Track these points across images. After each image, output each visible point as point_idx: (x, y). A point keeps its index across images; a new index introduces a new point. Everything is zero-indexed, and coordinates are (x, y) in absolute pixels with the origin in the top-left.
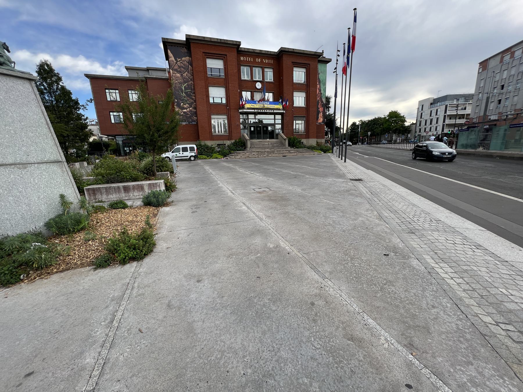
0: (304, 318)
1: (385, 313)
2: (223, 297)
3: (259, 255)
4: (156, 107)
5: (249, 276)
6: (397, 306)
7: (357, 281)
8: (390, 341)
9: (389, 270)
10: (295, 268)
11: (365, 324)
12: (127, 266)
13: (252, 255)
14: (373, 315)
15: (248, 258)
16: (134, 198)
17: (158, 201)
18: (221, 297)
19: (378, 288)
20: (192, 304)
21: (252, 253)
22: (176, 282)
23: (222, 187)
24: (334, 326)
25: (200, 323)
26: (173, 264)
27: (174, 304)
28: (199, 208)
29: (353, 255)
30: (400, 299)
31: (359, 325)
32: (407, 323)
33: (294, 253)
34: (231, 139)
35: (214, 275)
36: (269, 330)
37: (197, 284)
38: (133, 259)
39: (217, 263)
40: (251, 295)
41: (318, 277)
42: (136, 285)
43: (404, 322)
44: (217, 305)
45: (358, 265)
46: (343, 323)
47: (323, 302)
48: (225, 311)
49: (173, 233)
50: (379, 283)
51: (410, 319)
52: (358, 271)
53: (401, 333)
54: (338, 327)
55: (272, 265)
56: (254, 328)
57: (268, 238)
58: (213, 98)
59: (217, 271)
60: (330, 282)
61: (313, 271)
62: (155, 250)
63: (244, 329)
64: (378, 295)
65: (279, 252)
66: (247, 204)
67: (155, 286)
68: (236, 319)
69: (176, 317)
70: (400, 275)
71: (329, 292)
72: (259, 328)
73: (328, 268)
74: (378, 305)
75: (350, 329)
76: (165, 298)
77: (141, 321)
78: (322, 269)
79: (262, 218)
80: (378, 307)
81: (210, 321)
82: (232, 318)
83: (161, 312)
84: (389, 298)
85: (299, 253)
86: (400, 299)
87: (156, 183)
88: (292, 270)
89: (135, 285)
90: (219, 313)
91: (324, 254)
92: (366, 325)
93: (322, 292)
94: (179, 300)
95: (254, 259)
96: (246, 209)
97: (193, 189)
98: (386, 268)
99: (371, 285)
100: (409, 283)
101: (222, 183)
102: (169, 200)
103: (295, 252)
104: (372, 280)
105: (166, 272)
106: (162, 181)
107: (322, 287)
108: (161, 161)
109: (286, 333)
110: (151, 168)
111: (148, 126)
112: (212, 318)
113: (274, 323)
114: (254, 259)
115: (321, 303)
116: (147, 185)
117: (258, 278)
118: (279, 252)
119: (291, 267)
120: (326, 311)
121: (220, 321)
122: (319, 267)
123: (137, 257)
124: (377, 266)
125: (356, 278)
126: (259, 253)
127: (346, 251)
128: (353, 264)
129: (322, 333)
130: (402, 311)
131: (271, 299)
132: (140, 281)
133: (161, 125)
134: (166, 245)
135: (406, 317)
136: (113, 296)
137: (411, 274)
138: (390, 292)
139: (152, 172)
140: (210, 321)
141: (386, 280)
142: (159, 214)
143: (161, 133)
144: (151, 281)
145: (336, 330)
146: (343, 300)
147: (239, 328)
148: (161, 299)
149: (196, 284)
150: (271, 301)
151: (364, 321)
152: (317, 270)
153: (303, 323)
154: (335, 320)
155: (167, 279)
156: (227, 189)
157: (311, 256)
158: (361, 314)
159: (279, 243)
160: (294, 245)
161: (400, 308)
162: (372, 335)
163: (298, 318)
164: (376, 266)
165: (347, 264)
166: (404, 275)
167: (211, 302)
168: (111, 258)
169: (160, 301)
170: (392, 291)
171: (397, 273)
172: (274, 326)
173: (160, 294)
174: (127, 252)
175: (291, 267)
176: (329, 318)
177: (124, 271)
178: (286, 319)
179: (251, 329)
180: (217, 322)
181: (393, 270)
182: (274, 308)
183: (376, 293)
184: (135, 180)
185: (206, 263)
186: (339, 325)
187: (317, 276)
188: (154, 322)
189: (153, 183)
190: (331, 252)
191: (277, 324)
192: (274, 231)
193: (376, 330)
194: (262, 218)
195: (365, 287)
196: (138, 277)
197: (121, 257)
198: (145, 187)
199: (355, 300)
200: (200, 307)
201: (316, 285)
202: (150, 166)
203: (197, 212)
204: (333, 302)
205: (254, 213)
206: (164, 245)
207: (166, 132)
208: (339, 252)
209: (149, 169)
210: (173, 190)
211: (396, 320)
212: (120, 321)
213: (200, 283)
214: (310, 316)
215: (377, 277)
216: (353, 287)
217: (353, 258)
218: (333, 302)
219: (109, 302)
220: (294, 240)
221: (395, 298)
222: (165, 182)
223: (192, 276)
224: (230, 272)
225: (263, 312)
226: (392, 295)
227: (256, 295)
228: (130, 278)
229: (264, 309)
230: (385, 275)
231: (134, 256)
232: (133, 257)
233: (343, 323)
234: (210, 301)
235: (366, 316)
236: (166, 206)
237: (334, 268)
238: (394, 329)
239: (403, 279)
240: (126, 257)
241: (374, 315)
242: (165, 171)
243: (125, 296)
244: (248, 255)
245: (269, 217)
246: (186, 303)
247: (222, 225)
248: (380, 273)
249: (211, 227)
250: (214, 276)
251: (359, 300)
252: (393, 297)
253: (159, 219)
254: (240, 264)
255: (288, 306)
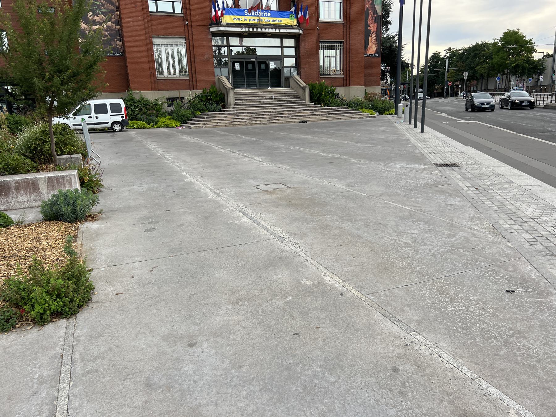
0: (383, 391)
1: (514, 378)
2: (240, 367)
3: (290, 298)
4: (52, 24)
5: (279, 333)
6: (534, 367)
7: (465, 334)
8: (525, 415)
9: (517, 314)
10: (357, 317)
11: (484, 395)
12: (49, 328)
13: (278, 300)
14: (496, 381)
15: (271, 304)
16: (20, 207)
17: (74, 211)
18: (237, 366)
19: (501, 342)
20: (190, 380)
21: (276, 295)
22: (150, 349)
23: (192, 183)
24: (434, 400)
25: (212, 408)
26: (136, 320)
27: (157, 382)
28: (156, 222)
29: (454, 294)
30: (536, 357)
31: (475, 396)
32: (549, 390)
33: (351, 294)
34: (348, 84)
35: (215, 334)
36: (330, 410)
37: (191, 350)
38: (58, 315)
39: (217, 315)
40: (289, 362)
41: (399, 330)
42: (77, 356)
43: (544, 389)
44: (234, 380)
45: (464, 308)
46: (448, 395)
47: (412, 366)
48: (249, 388)
49: (120, 268)
50: (501, 334)
51: (553, 383)
52: (466, 317)
53: (540, 403)
54: (441, 401)
55: (317, 314)
56: (305, 409)
57: (299, 271)
58: (173, 2)
59: (221, 327)
60: (419, 337)
61: (388, 320)
62: (94, 298)
63: (289, 411)
64: (502, 353)
65: (323, 292)
66: (249, 212)
67: (114, 357)
68: (271, 399)
69: (167, 401)
70: (536, 321)
71: (420, 351)
72: (313, 409)
73: (413, 315)
74: (502, 367)
75: (461, 402)
76: (138, 374)
77: (106, 411)
78: (404, 318)
79: (282, 236)
80: (503, 370)
81: (228, 403)
82: (264, 397)
83: (138, 396)
84: (519, 356)
85: (359, 294)
86: (536, 357)
87: (63, 177)
88: (353, 320)
89: (76, 356)
90: (240, 392)
91: (403, 294)
92: (486, 396)
93: (408, 351)
94: (164, 376)
95: (282, 305)
96: (249, 221)
97: (135, 187)
98: (512, 312)
99: (489, 339)
100: (550, 333)
101: (190, 175)
102: (95, 209)
103: (352, 291)
104: (490, 331)
105: (127, 333)
106: (75, 172)
107: (407, 345)
108: (61, 134)
109: (358, 413)
110: (40, 146)
111: (40, 62)
112: (229, 398)
113: (336, 401)
114: (282, 305)
115: (409, 367)
116: (45, 181)
117: (296, 335)
118: (323, 292)
119: (349, 316)
120: (419, 379)
121: (245, 403)
122: (398, 314)
123: (66, 312)
124: (496, 309)
125: (463, 329)
126: (290, 296)
127: (442, 287)
128: (455, 307)
129: (417, 411)
130: (541, 373)
131: (324, 366)
132: (84, 351)
133: (66, 60)
134: (112, 289)
135: (547, 382)
136: (41, 377)
137: (552, 319)
138: (521, 347)
139: (42, 154)
140: (228, 403)
141: (513, 330)
142: (80, 235)
143: (65, 75)
144: (103, 349)
145: (439, 404)
146: (445, 361)
147: (280, 410)
148: (131, 376)
149: (187, 349)
150: (325, 368)
151: (481, 390)
152: (396, 319)
153: (385, 398)
154: (436, 391)
155: (133, 344)
156: (203, 187)
157: (382, 298)
158: (476, 380)
159: (322, 278)
160: (349, 280)
161: (537, 369)
162: (496, 409)
163: (375, 391)
164: (495, 310)
165: (445, 307)
166: (542, 321)
167: (222, 375)
168: (15, 314)
169: (130, 379)
170: (524, 346)
171: (530, 319)
172: (337, 405)
173: (126, 368)
174: (46, 302)
175: (349, 316)
176: (425, 388)
177: (45, 335)
178: (355, 393)
179: (300, 410)
180: (240, 405)
181: (523, 314)
182: (332, 379)
183: (497, 349)
184: (14, 171)
185: (197, 315)
186: (442, 397)
187: (396, 328)
188: (129, 410)
189: (57, 178)
190: (416, 289)
191: (342, 402)
192: (309, 259)
193: (502, 402)
194: (282, 236)
195: (478, 342)
196: (77, 344)
197: (36, 311)
198: (40, 184)
199: (464, 361)
200: (204, 384)
201: (398, 342)
202: (39, 142)
203: (155, 229)
204: (428, 366)
205: (266, 229)
206: (110, 289)
207: (75, 75)
208: (430, 289)
209: (35, 149)
210: (95, 189)
211: (532, 386)
212: (68, 413)
213: (194, 348)
214: (393, 388)
215: (497, 325)
216: (459, 343)
217: (455, 298)
218: (428, 366)
219: (36, 386)
220: (347, 272)
221: (529, 355)
222: (79, 175)
223: (176, 338)
224: (244, 327)
225: (315, 386)
226: (524, 351)
227: (298, 361)
228: (62, 347)
229: (316, 381)
230: (510, 322)
231: (60, 310)
232: (57, 311)
233: (448, 395)
234: (219, 373)
235: (484, 384)
236: (90, 221)
237: (424, 315)
238: (529, 399)
239: (540, 327)
240: (45, 311)
241: (498, 381)
242: (69, 153)
243: (63, 375)
244: (270, 300)
245: (295, 234)
246: (178, 379)
247: (211, 251)
248: (501, 320)
249: (191, 255)
250: (218, 336)
251: (472, 361)
252: (525, 355)
253: (84, 243)
254: (260, 315)
255: (355, 375)
